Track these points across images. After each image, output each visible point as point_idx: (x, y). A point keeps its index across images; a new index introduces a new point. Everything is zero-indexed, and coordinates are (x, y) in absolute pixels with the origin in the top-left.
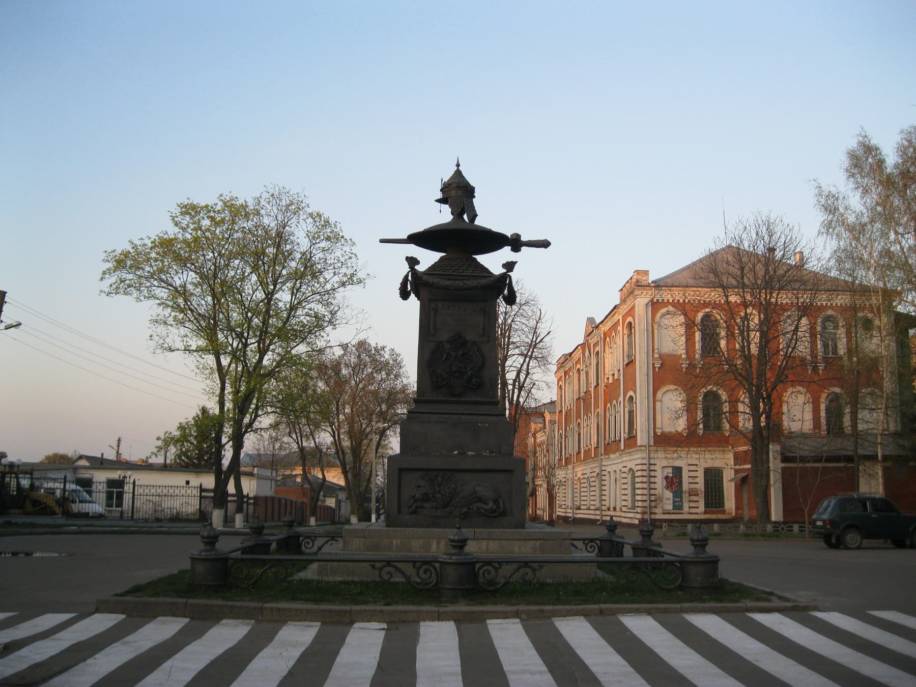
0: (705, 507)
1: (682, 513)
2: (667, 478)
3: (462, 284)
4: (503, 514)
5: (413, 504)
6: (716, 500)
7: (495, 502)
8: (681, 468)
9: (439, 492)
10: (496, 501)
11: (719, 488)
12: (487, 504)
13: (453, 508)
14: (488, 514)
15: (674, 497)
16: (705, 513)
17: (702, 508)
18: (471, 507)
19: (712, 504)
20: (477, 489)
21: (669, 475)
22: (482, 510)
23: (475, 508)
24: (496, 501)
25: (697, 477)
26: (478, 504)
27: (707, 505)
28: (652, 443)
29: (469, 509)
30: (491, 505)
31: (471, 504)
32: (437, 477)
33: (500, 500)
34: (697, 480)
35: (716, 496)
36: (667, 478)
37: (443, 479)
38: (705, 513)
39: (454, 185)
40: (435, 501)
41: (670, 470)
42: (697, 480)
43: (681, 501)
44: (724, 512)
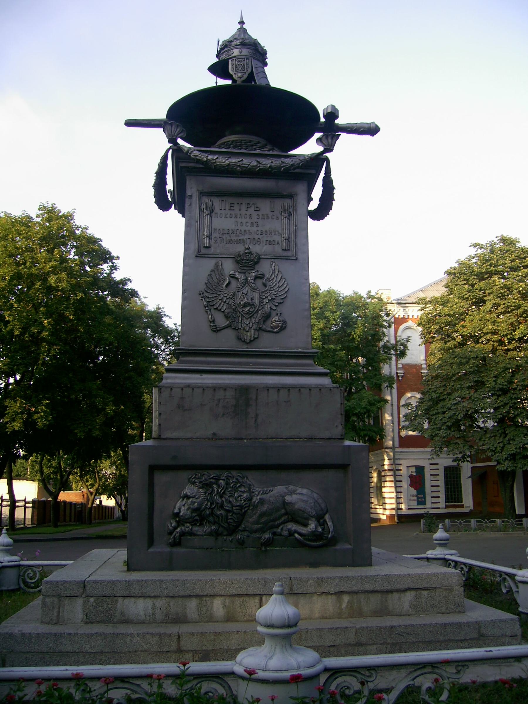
0: (446, 502)
1: (425, 508)
2: (411, 476)
3: (254, 163)
4: (332, 542)
5: (175, 528)
6: (455, 495)
7: (318, 521)
8: (423, 467)
9: (222, 506)
10: (320, 519)
11: (457, 485)
12: (306, 525)
13: (246, 534)
14: (312, 543)
15: (418, 494)
16: (447, 507)
17: (443, 504)
18: (279, 530)
19: (452, 499)
20: (288, 498)
21: (413, 473)
22: (296, 535)
23: (285, 533)
24: (320, 519)
25: (438, 475)
26: (292, 526)
27: (447, 500)
28: (397, 444)
29: (274, 534)
30: (312, 526)
31: (278, 526)
32: (217, 479)
33: (327, 517)
34: (438, 478)
35: (455, 492)
36: (411, 476)
37: (227, 484)
38: (447, 507)
39: (238, 42)
40: (215, 523)
41: (414, 469)
42: (438, 478)
43: (424, 497)
44: (462, 506)
